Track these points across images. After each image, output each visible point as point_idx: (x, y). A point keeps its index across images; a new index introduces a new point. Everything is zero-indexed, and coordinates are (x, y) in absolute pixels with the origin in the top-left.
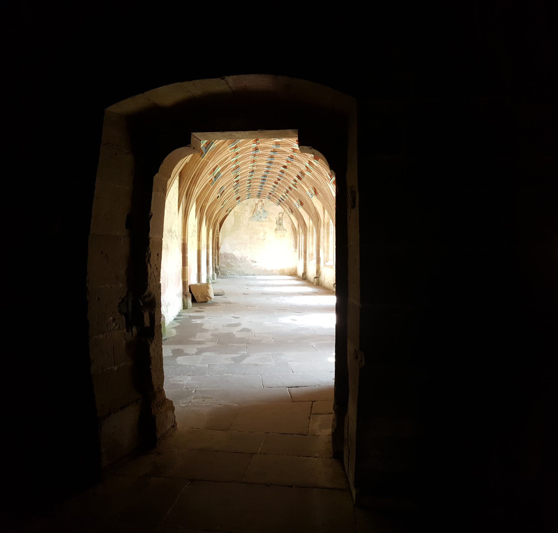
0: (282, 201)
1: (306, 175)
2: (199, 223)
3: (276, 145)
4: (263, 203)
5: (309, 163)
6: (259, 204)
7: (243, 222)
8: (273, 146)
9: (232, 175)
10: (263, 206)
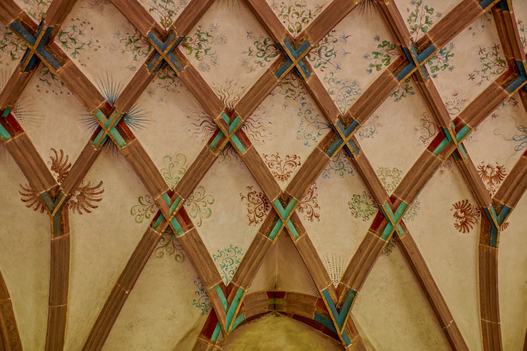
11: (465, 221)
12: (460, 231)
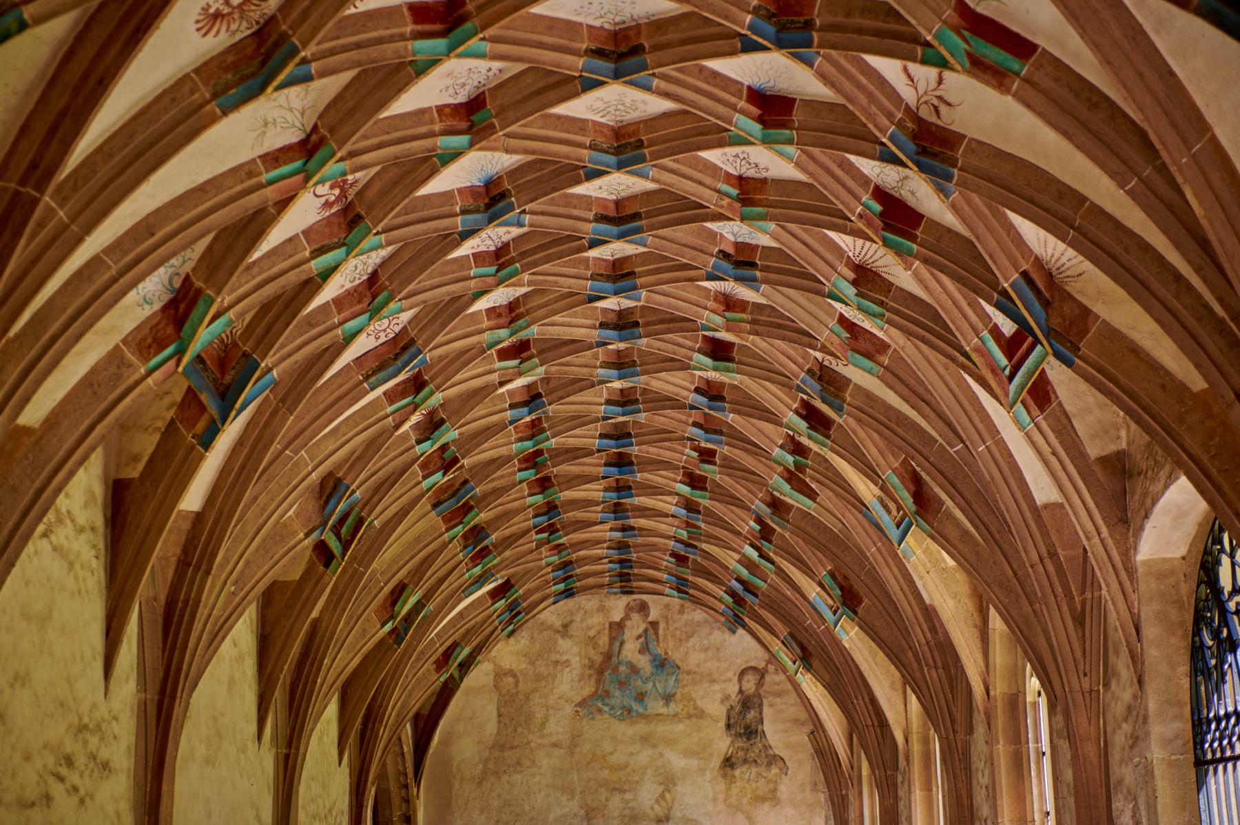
0: (749, 598)
1: (851, 387)
2: (152, 710)
3: (617, 151)
4: (650, 619)
5: (854, 283)
6: (628, 623)
7: (543, 725)
8: (594, 153)
9: (389, 410)
10: (651, 631)
11: (223, 16)
12: (198, 22)
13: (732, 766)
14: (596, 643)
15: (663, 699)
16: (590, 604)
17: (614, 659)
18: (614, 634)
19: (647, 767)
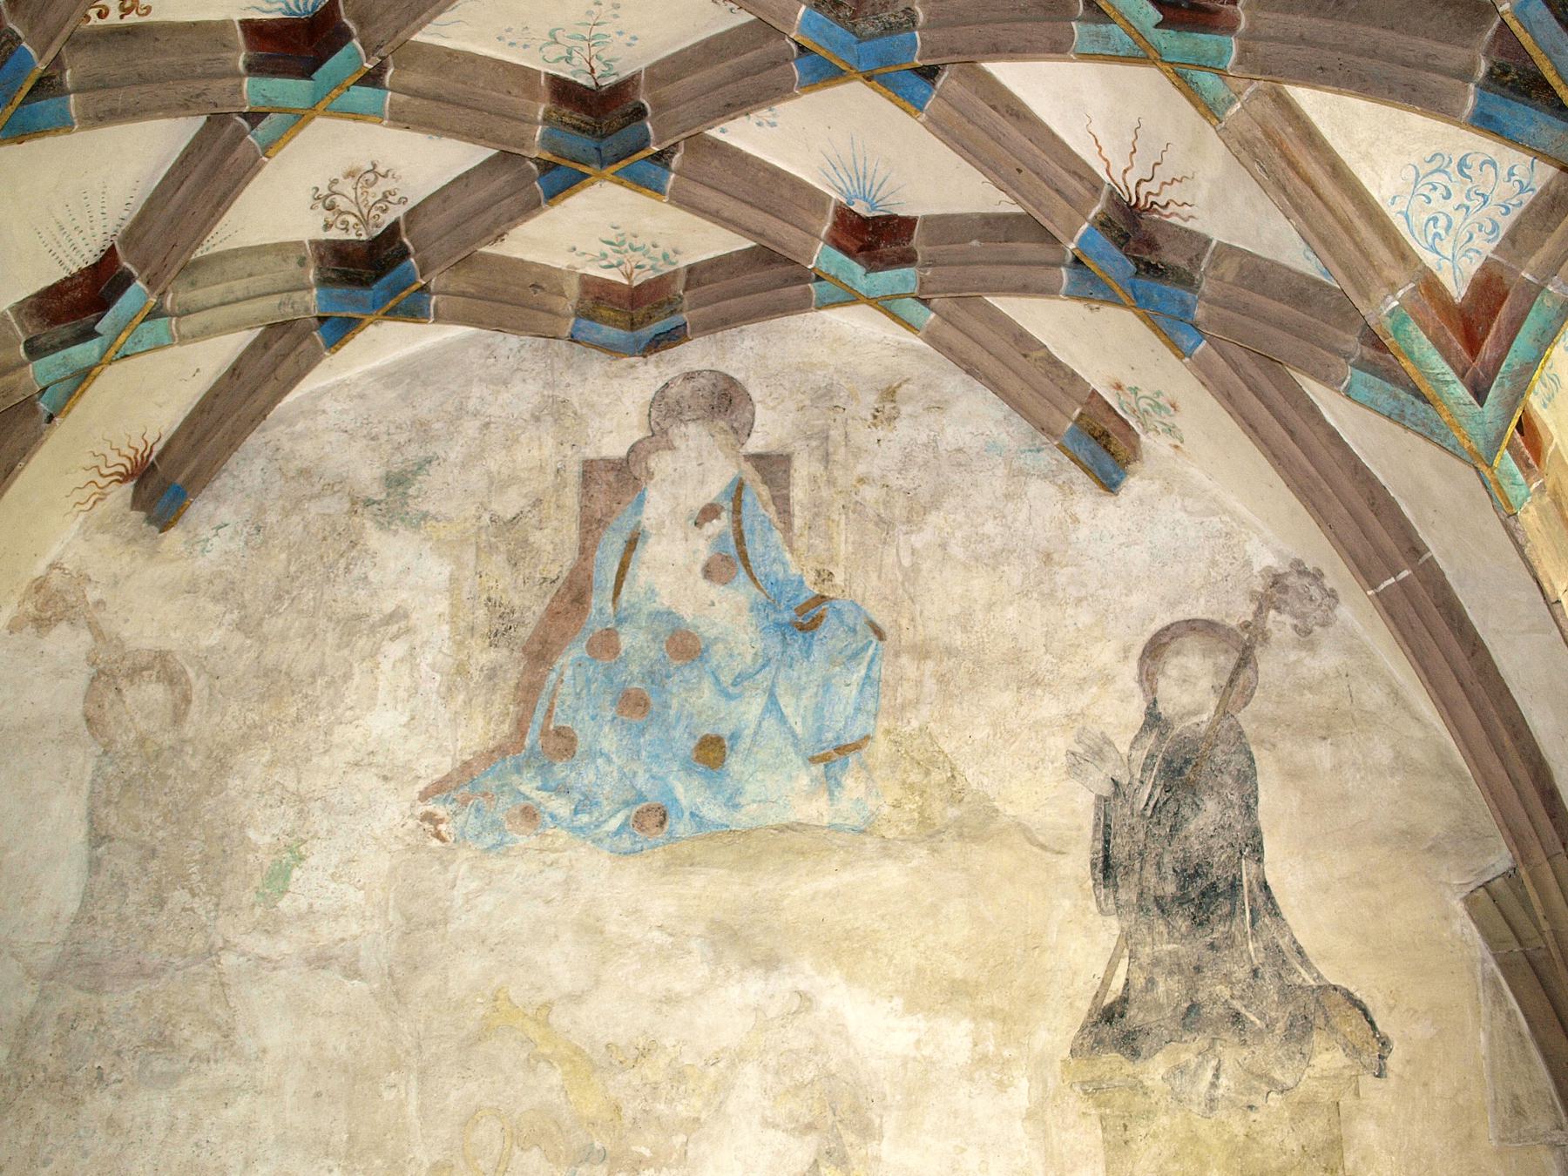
4: (755, 444)
6: (661, 464)
7: (279, 877)
13: (1130, 1044)
14: (524, 543)
15: (813, 760)
16: (505, 396)
17: (600, 601)
18: (600, 505)
19: (740, 1056)
